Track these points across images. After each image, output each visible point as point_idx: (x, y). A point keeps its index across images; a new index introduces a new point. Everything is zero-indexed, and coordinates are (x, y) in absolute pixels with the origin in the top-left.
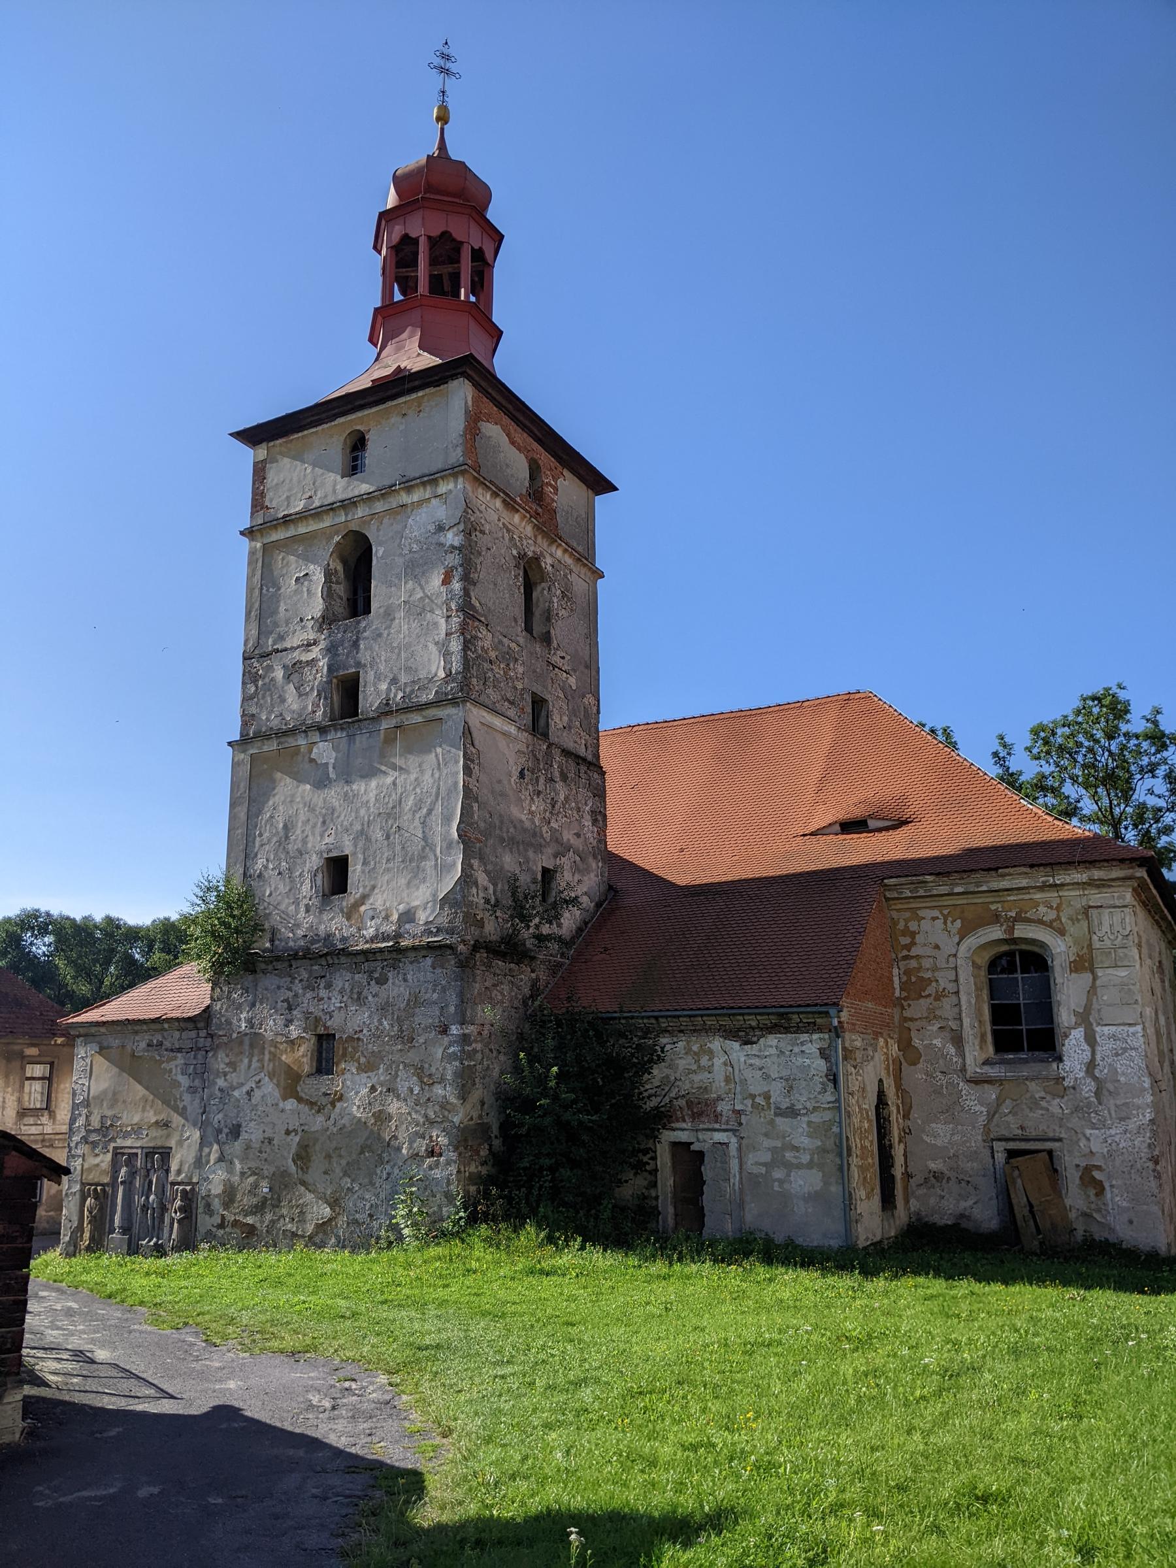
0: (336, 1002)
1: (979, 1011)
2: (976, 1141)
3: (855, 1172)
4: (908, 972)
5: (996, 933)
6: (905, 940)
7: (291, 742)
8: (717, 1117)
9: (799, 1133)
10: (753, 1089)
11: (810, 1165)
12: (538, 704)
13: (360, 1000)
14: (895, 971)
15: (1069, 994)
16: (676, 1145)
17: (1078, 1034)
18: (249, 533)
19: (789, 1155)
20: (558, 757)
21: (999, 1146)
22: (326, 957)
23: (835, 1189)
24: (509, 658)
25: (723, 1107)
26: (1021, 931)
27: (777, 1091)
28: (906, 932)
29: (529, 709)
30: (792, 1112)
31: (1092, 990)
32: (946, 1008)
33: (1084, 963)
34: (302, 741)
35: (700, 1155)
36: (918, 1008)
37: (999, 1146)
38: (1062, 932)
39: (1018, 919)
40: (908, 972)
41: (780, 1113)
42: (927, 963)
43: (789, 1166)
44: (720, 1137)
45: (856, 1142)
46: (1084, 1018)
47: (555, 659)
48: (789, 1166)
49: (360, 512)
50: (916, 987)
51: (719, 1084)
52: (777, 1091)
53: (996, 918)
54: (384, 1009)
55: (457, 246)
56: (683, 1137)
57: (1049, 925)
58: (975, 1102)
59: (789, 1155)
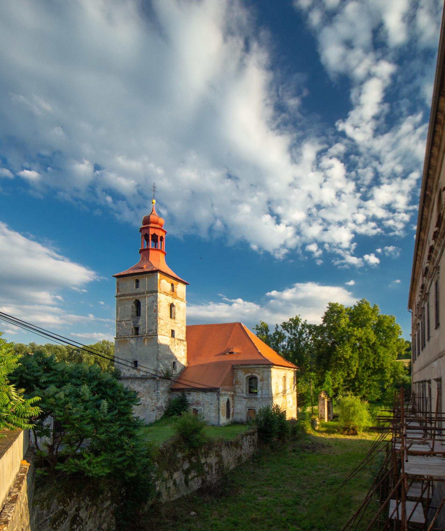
0: (136, 386)
1: (246, 387)
2: (244, 407)
3: (221, 413)
4: (236, 380)
5: (250, 374)
6: (236, 375)
7: (126, 339)
8: (200, 405)
9: (213, 407)
10: (207, 400)
11: (214, 412)
12: (173, 331)
13: (140, 386)
14: (234, 380)
15: (260, 384)
16: (194, 409)
17: (260, 391)
18: (116, 297)
19: (211, 411)
20: (176, 340)
21: (247, 408)
22: (134, 378)
23: (217, 416)
24: (167, 324)
25: (201, 403)
26: (254, 374)
27: (210, 401)
28: (236, 374)
29: (171, 333)
30: (212, 404)
31: (263, 384)
32: (241, 387)
33: (262, 380)
34: (128, 339)
35: (197, 410)
36: (237, 386)
37: (247, 408)
38: (259, 375)
39: (253, 372)
40: (236, 380)
41: (210, 404)
42: (239, 379)
43: (211, 412)
44: (200, 408)
45: (221, 409)
46: (261, 389)
47: (176, 322)
48: (211, 412)
49: (138, 296)
50: (237, 383)
51: (201, 400)
52: (210, 401)
53: (250, 372)
54: (145, 387)
55: (157, 236)
56: (195, 408)
57: (258, 373)
58: (244, 402)
59: (211, 411)
